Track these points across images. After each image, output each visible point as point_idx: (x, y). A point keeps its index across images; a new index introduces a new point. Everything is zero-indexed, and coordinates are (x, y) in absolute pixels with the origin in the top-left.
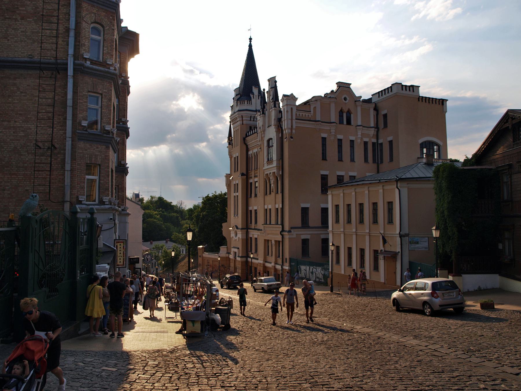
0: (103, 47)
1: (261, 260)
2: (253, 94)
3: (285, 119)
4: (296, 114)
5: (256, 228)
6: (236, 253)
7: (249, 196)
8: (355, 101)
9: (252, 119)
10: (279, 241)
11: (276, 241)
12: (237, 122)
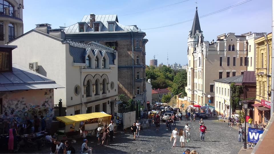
7: (194, 77)
11: (201, 97)
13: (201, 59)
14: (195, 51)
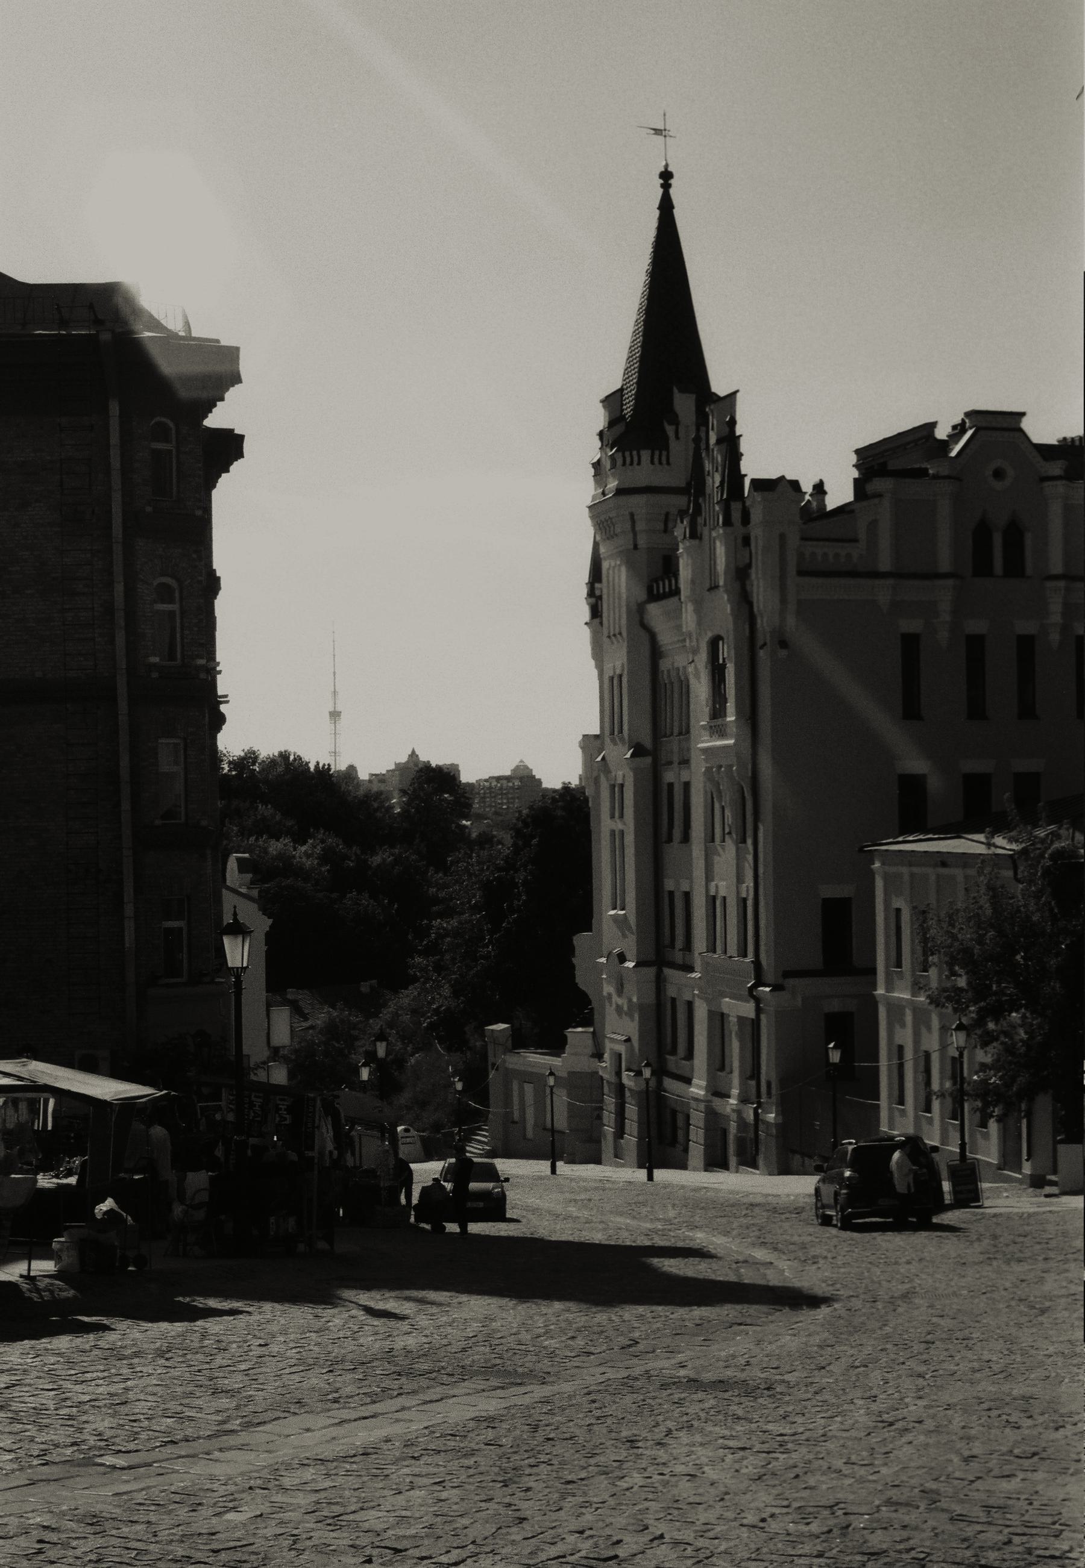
0: (182, 629)
1: (699, 1087)
2: (675, 421)
11: (741, 1019)
14: (664, 587)
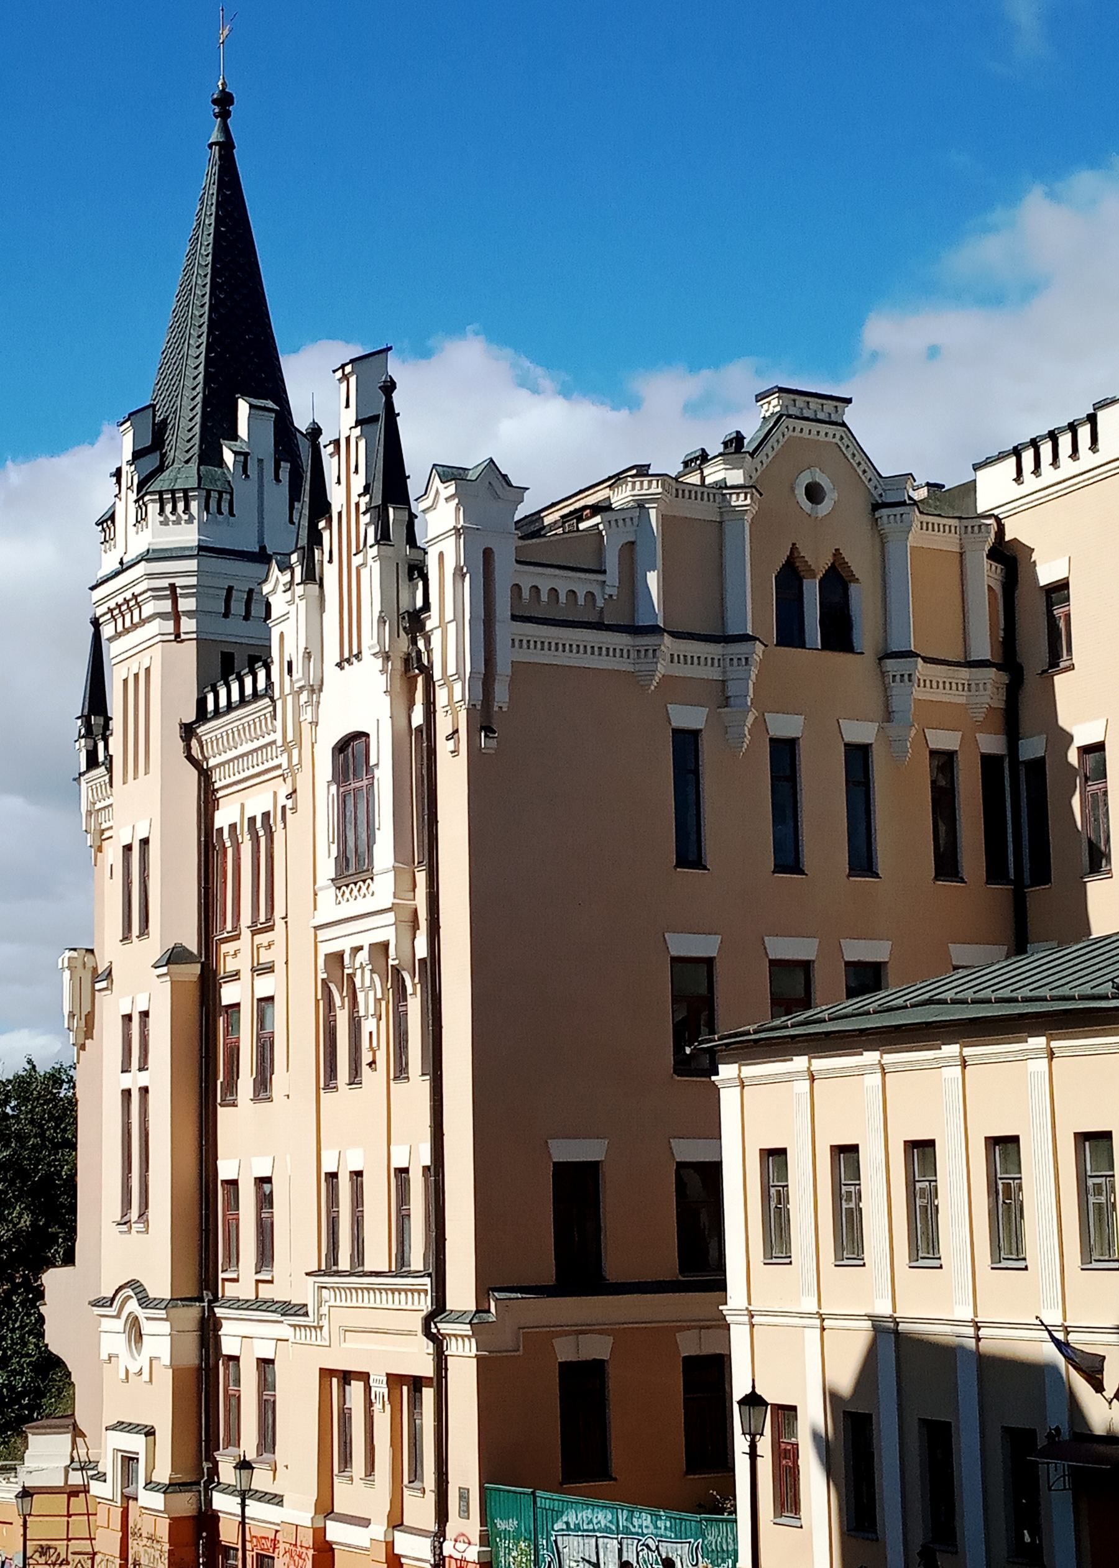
3: (449, 615)
4: (517, 588)
5: (266, 1292)
6: (129, 1460)
8: (876, 507)
9: (238, 608)
10: (417, 1383)
11: (395, 1380)
12: (143, 622)
13: (382, 754)
